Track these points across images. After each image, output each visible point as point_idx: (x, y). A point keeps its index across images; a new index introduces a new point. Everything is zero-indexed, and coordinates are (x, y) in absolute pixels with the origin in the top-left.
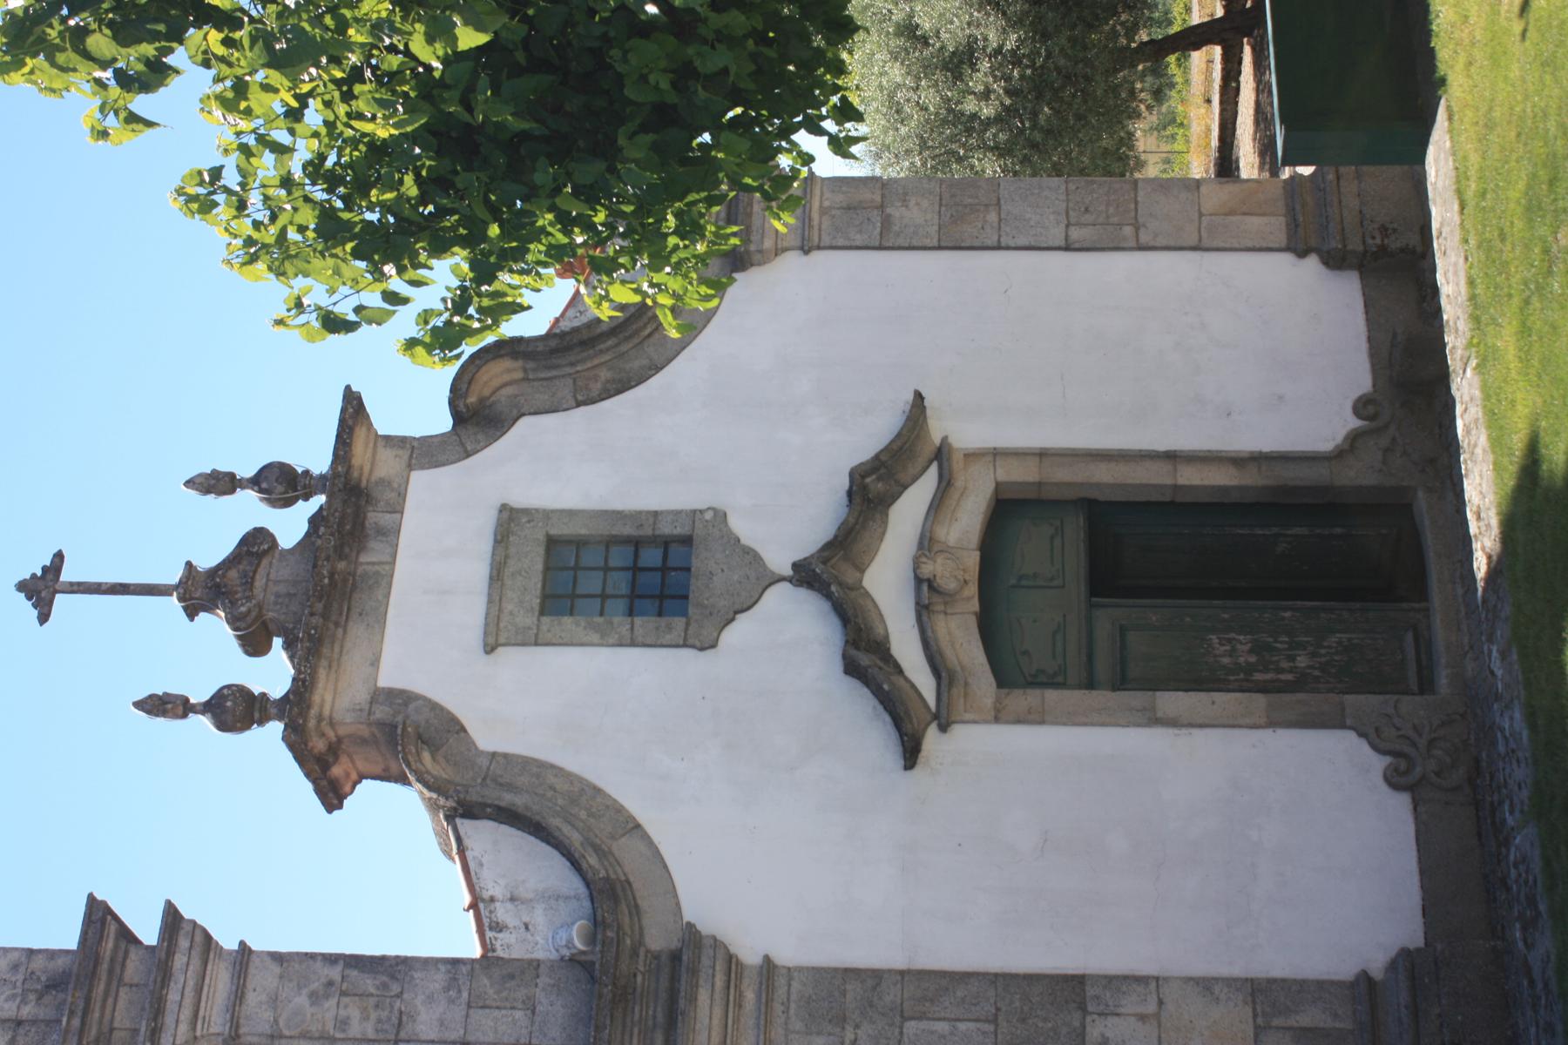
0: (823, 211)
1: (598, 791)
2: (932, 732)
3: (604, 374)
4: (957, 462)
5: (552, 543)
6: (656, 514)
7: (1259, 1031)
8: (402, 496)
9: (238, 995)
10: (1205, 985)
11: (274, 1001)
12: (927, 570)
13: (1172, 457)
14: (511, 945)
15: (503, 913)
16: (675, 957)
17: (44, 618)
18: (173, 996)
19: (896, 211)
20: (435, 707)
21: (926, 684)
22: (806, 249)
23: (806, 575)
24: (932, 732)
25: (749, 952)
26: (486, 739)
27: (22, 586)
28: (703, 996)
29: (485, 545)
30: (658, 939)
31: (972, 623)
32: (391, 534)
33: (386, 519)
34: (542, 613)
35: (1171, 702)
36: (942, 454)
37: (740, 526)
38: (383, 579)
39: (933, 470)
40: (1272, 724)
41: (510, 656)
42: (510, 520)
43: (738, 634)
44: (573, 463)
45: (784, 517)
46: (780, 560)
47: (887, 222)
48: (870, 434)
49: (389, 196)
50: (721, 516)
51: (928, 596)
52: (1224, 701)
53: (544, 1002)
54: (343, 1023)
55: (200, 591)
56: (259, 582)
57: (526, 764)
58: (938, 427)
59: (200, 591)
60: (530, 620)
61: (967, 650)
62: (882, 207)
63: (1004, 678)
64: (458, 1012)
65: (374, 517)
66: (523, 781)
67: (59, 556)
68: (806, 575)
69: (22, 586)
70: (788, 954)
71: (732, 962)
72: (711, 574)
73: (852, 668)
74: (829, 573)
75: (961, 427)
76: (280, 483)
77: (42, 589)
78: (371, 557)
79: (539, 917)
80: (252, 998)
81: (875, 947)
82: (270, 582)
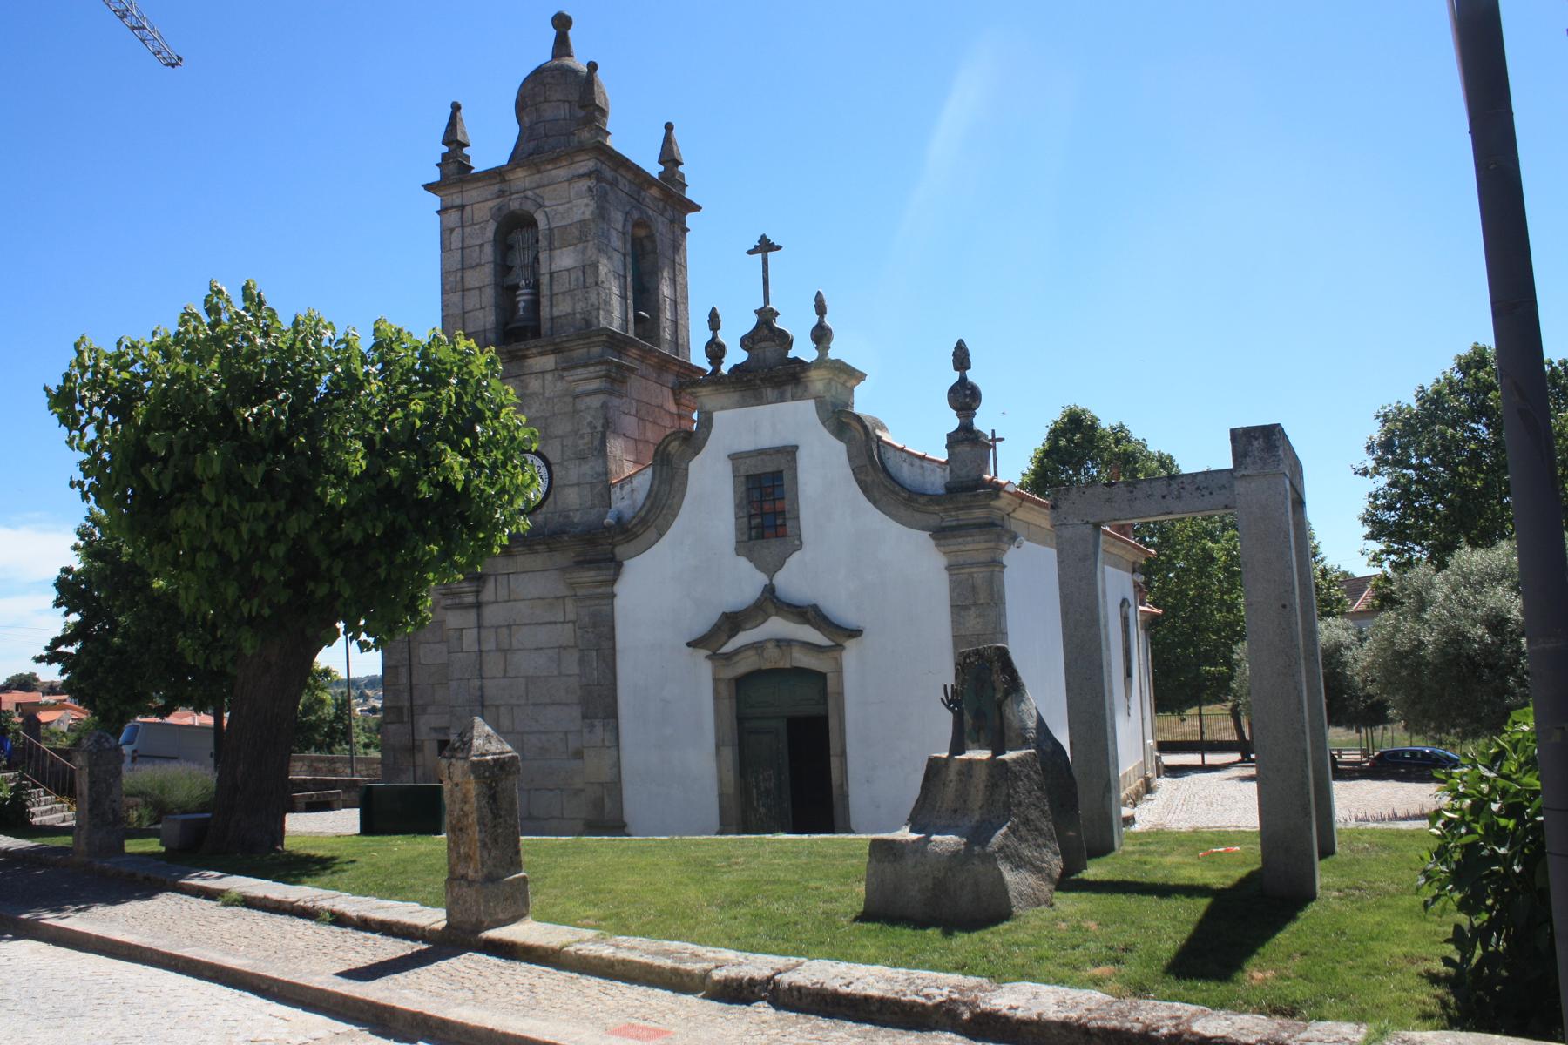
0: (971, 574)
1: (675, 516)
2: (708, 652)
3: (869, 479)
4: (836, 654)
5: (777, 476)
6: (797, 518)
7: (601, 784)
8: (800, 398)
9: (588, 394)
10: (617, 764)
11: (588, 408)
12: (770, 645)
13: (843, 754)
14: (616, 493)
15: (627, 488)
16: (613, 559)
17: (750, 252)
18: (580, 371)
19: (973, 612)
20: (705, 440)
21: (729, 647)
22: (949, 568)
23: (770, 590)
24: (708, 652)
25: (619, 588)
26: (694, 465)
27: (763, 237)
28: (592, 573)
29: (778, 443)
30: (619, 551)
31: (756, 667)
32: (782, 399)
33: (789, 395)
34: (748, 477)
35: (729, 754)
36: (839, 647)
37: (796, 555)
38: (760, 400)
39: (829, 643)
40: (721, 796)
41: (729, 464)
42: (789, 453)
43: (744, 563)
44: (823, 471)
45: (794, 580)
46: (761, 579)
47: (966, 608)
48: (842, 609)
49: (237, 506)
50: (800, 547)
51: (783, 644)
52: (730, 777)
53: (594, 512)
54: (582, 437)
55: (766, 316)
56: (763, 345)
57: (685, 484)
58: (851, 645)
59: (766, 316)
60: (742, 472)
61: (744, 666)
62: (975, 604)
63: (741, 682)
64: (589, 479)
65: (789, 389)
66: (676, 484)
67: (779, 248)
68: (770, 590)
69: (763, 237)
70: (618, 602)
71: (614, 581)
72: (773, 547)
73: (815, 608)
74: (770, 602)
75: (852, 654)
76: (821, 335)
77: (765, 246)
78: (770, 392)
79: (627, 502)
80: (587, 400)
81: (625, 636)
82: (769, 350)
